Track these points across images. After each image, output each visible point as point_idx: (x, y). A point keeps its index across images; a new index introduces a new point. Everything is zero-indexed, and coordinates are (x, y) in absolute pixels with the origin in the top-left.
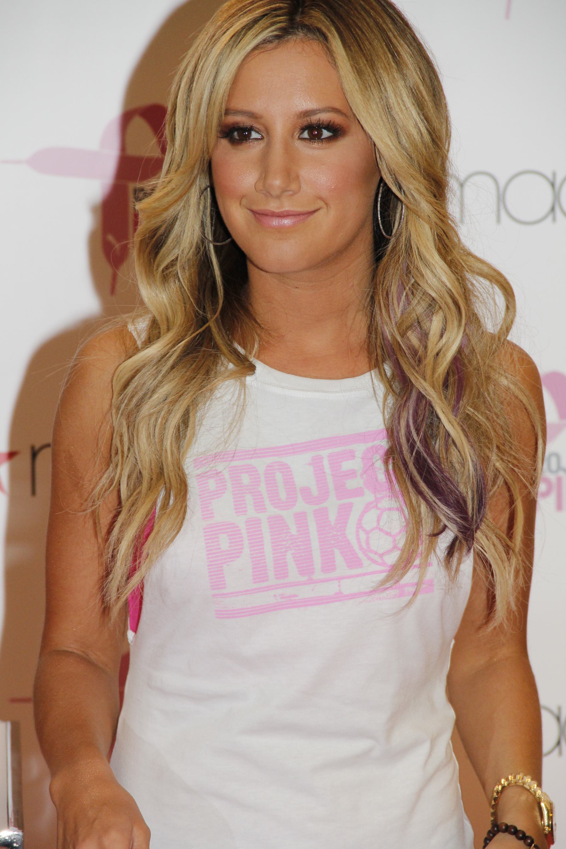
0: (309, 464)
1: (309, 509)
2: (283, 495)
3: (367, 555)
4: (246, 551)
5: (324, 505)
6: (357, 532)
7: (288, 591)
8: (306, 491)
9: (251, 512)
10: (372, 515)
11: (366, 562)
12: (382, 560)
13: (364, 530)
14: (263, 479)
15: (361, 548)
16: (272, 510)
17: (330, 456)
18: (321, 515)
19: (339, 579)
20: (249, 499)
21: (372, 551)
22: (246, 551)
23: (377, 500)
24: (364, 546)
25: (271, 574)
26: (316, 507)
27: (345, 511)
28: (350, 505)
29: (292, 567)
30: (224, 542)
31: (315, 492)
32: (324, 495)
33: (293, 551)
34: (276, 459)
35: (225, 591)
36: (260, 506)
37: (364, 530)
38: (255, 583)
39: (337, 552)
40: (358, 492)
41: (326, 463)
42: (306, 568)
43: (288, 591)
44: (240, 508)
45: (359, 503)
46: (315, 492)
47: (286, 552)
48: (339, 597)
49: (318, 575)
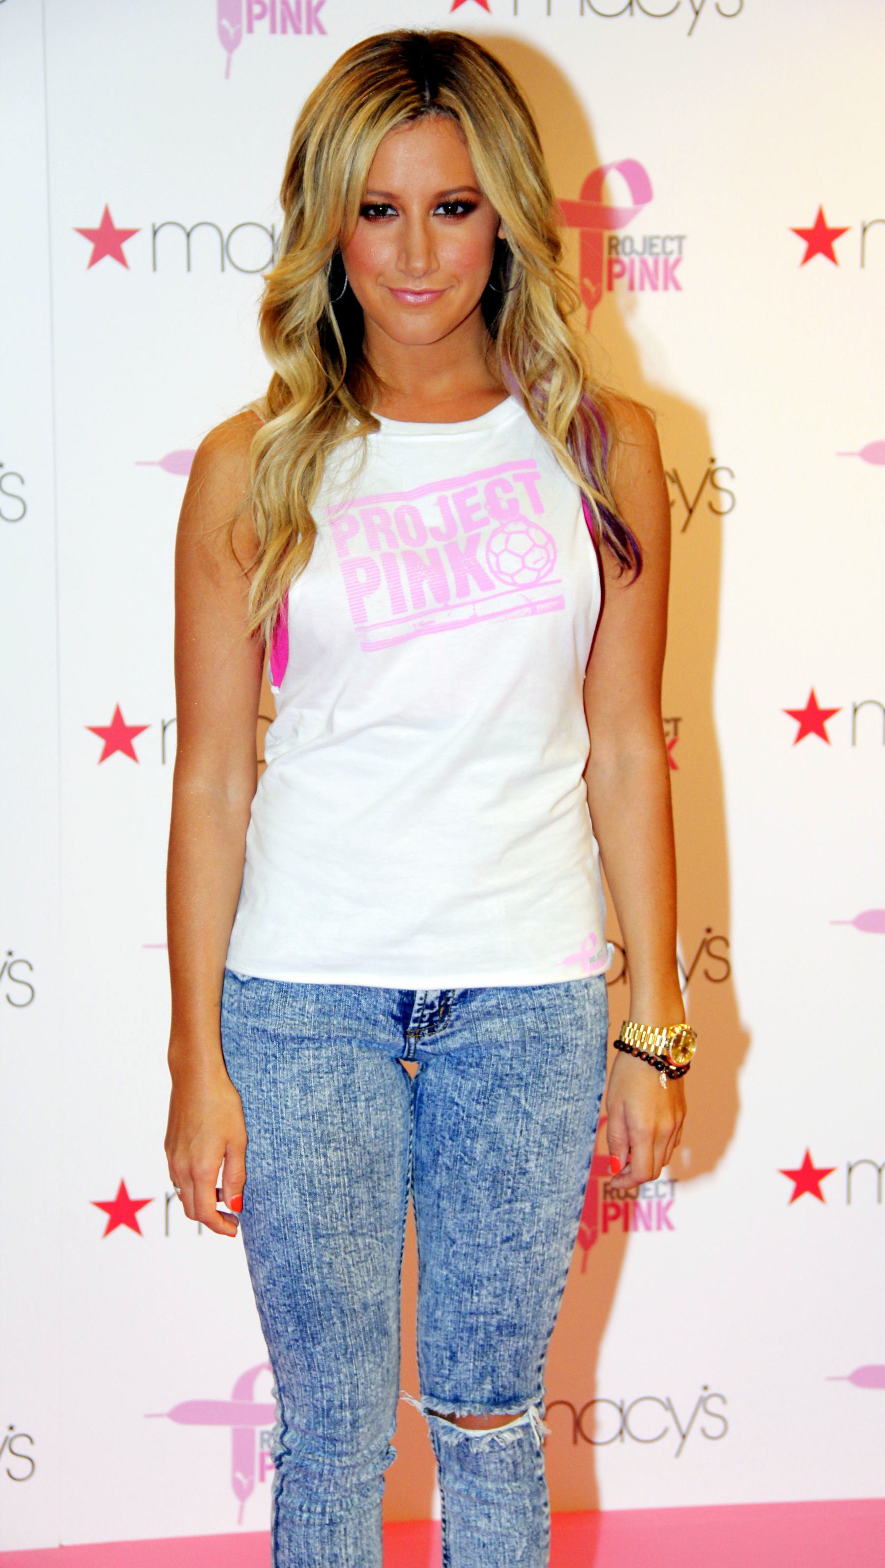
0: (436, 505)
1: (439, 545)
2: (413, 534)
3: (497, 577)
4: (384, 583)
5: (454, 539)
6: (487, 555)
7: (425, 619)
8: (435, 532)
9: (385, 547)
10: (501, 538)
11: (496, 582)
12: (513, 580)
13: (494, 553)
14: (393, 520)
15: (492, 570)
16: (403, 546)
17: (454, 496)
18: (452, 550)
19: (474, 602)
20: (382, 537)
21: (502, 573)
22: (384, 583)
23: (503, 526)
24: (495, 569)
25: (409, 604)
26: (447, 542)
27: (473, 542)
28: (479, 535)
29: (429, 596)
30: (362, 576)
31: (444, 530)
32: (452, 529)
33: (428, 580)
34: (404, 503)
35: (366, 624)
36: (392, 542)
37: (494, 553)
38: (394, 614)
39: (470, 577)
40: (485, 522)
41: (451, 502)
42: (442, 595)
43: (425, 619)
44: (374, 544)
45: (486, 531)
46: (444, 530)
47: (421, 581)
48: (474, 619)
49: (454, 600)
